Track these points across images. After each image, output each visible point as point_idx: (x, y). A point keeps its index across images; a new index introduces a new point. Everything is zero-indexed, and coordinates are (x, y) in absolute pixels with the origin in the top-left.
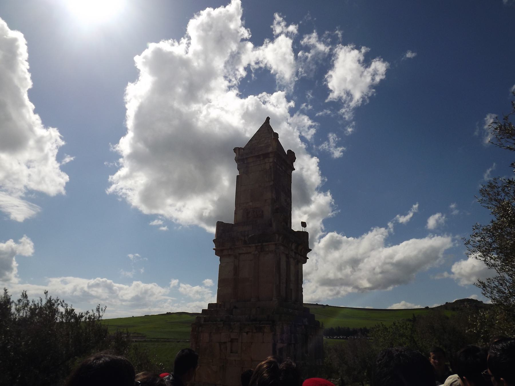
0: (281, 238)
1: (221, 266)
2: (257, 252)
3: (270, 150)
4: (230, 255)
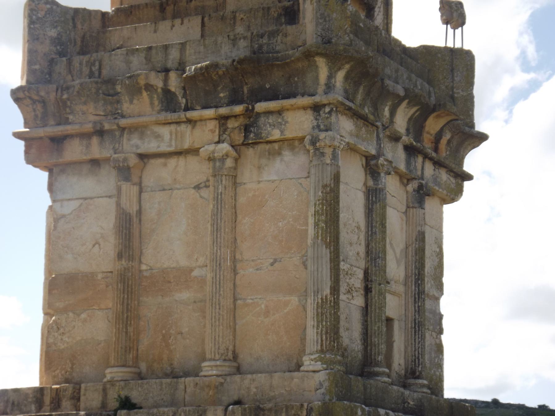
0: (340, 76)
2: (225, 147)
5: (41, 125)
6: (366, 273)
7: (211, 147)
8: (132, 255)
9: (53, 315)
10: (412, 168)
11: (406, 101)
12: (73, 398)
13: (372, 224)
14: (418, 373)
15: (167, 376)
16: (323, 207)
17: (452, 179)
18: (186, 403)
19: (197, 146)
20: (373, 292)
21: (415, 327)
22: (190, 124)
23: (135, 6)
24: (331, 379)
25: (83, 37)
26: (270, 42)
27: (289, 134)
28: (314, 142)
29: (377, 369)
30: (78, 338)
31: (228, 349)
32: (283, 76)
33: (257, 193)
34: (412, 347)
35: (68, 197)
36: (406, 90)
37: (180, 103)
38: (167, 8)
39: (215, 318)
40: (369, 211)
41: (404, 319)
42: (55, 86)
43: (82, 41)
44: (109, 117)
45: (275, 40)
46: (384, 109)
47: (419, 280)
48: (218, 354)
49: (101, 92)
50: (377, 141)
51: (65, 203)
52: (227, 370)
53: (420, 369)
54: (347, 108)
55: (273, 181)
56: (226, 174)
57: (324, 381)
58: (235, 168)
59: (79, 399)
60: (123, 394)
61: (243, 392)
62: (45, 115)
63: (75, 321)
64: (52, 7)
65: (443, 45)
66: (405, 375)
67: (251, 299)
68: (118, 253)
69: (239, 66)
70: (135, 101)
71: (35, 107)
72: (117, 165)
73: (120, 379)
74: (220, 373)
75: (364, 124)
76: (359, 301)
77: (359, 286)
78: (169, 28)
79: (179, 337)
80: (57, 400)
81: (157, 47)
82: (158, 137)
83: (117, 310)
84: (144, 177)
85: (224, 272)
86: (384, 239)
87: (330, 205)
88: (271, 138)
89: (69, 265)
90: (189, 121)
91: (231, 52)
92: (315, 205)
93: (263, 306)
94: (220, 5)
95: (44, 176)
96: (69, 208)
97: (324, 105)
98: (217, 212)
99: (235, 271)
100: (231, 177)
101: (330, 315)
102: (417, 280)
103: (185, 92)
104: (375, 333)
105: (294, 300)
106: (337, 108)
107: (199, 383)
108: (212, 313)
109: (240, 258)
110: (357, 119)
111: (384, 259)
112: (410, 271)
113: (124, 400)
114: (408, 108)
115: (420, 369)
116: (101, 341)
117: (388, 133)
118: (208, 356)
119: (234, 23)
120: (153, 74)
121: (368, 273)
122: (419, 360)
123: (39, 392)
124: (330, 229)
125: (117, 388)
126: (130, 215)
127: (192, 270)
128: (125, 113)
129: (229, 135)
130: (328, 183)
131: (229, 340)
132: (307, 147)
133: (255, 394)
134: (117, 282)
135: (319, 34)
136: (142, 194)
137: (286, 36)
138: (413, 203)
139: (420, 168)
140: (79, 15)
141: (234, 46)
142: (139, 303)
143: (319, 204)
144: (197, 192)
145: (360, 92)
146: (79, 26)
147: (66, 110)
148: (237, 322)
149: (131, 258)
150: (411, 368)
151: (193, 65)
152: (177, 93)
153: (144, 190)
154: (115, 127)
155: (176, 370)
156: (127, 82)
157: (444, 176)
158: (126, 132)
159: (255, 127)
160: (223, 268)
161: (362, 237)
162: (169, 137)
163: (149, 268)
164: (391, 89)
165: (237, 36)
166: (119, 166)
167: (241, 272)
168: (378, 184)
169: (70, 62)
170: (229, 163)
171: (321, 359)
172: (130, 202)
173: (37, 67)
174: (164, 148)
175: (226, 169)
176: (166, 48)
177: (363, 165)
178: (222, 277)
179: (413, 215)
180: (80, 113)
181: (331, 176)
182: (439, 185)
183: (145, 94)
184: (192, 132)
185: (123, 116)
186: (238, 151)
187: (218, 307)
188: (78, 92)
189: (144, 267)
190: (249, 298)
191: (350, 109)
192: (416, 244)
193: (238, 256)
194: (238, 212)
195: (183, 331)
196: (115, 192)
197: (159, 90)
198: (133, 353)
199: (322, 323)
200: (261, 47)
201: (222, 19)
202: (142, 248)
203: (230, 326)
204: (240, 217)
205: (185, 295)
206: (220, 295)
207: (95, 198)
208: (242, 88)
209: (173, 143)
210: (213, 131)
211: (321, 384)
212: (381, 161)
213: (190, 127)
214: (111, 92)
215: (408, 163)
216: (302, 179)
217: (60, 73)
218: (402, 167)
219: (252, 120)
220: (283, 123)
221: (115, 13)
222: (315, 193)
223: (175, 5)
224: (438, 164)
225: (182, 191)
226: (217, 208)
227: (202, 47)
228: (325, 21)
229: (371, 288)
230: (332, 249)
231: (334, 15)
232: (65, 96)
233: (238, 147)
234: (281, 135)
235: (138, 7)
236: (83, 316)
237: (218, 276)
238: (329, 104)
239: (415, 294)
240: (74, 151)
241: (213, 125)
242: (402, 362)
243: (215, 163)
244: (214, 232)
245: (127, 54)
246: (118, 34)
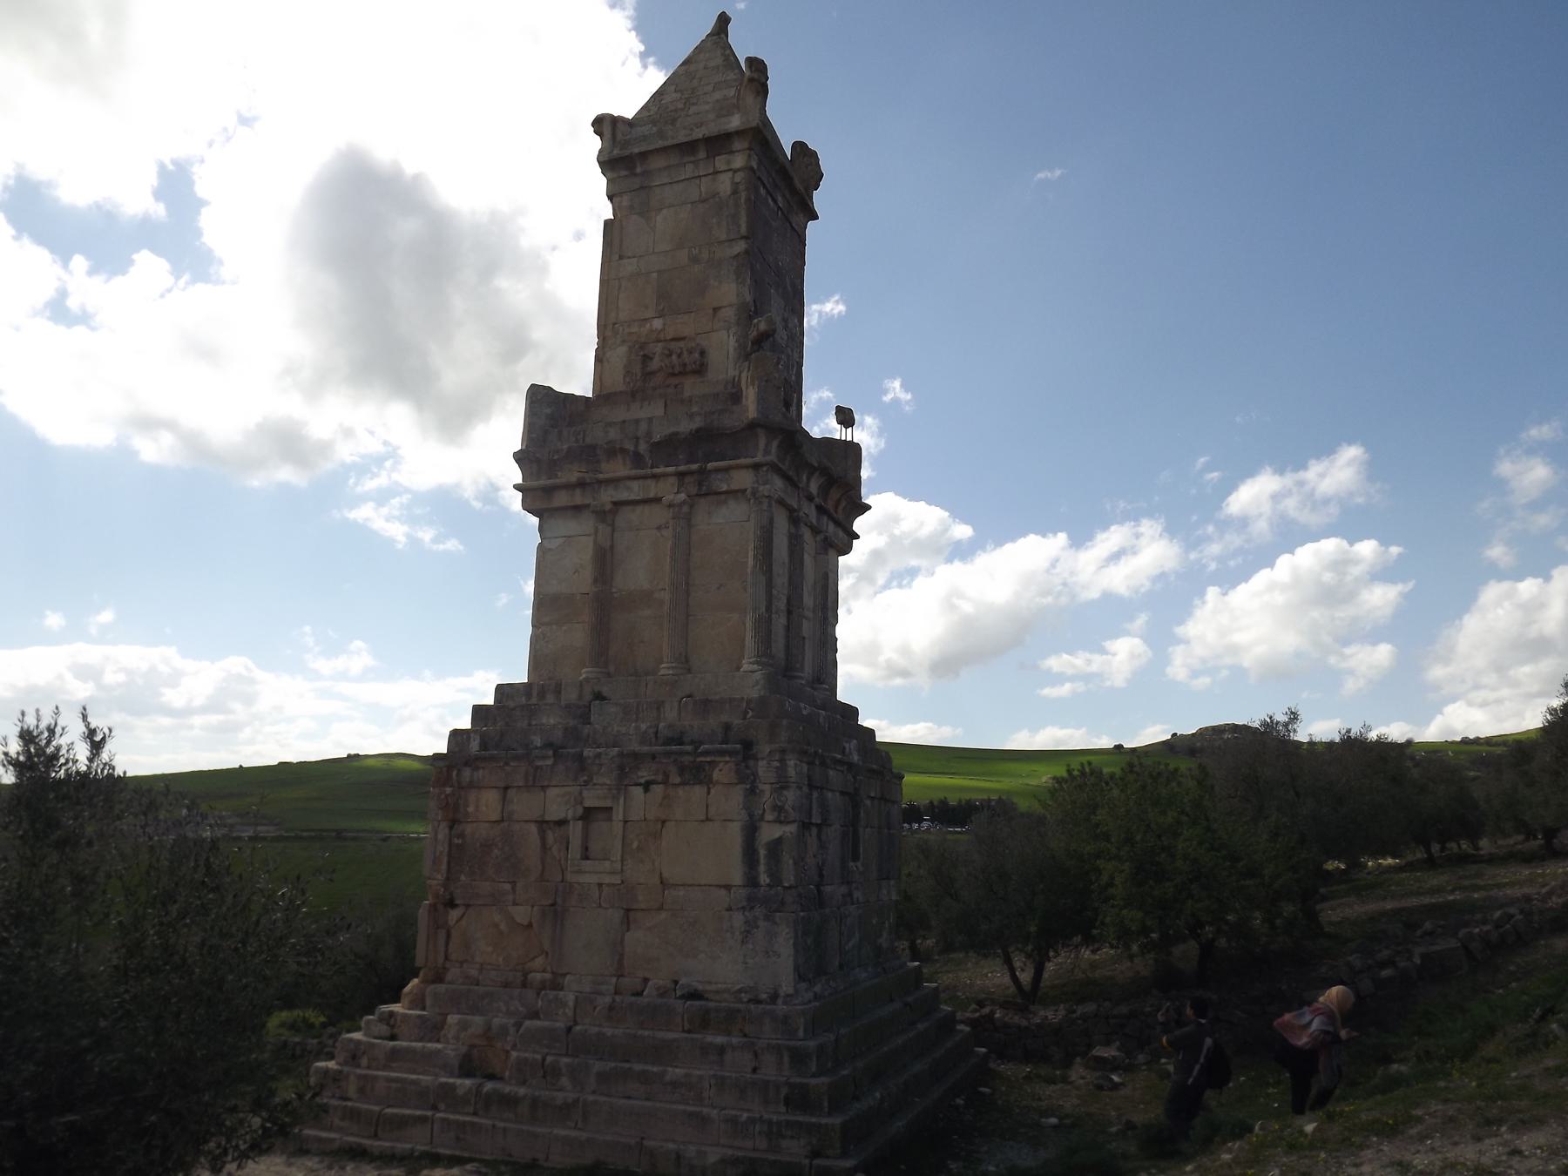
0: (775, 444)
3: (735, 122)
4: (578, 509)
27: (734, 486)
76: (783, 621)
90: (655, 477)
95: (535, 520)
123: (526, 688)
157: (841, 534)
170: (685, 509)
174: (633, 497)
176: (637, 421)
211: (757, 683)
215: (818, 519)
224: (837, 523)
240: (562, 499)
241: (673, 480)
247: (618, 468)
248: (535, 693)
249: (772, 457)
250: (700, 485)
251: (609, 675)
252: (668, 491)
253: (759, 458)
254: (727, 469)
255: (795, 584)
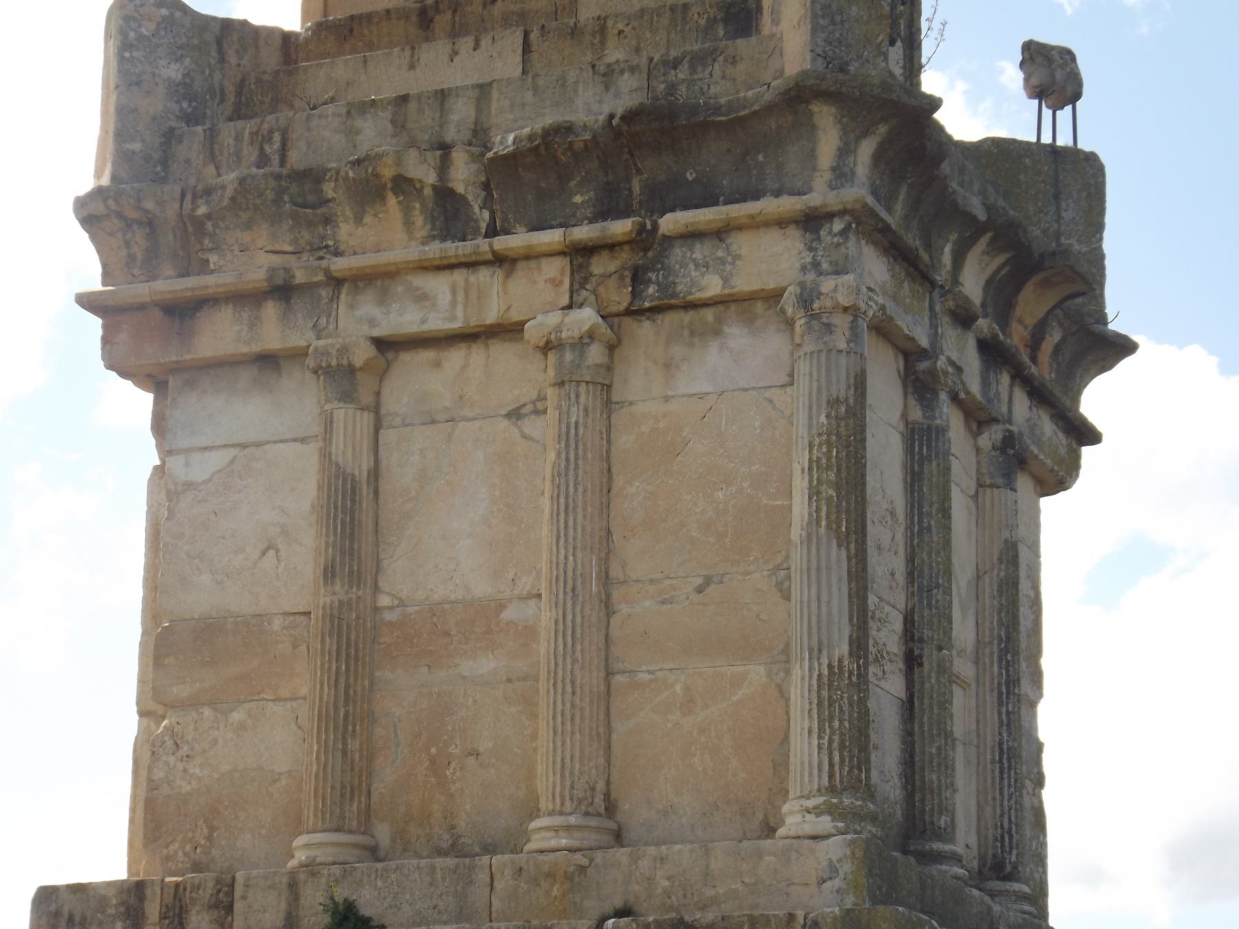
1: (167, 492)
2: (586, 317)
4: (268, 362)
5: (144, 278)
6: (909, 620)
7: (553, 319)
8: (359, 572)
9: (164, 718)
10: (992, 393)
11: (989, 235)
12: (215, 906)
13: (920, 507)
14: (1008, 868)
15: (441, 853)
16: (829, 451)
17: (1060, 435)
18: (494, 915)
19: (515, 316)
20: (926, 667)
21: (1001, 761)
22: (500, 266)
23: (360, 17)
24: (859, 854)
25: (241, 86)
26: (696, 77)
27: (743, 284)
28: (806, 300)
29: (937, 846)
30: (225, 768)
31: (593, 789)
32: (729, 150)
33: (661, 425)
34: (994, 808)
35: (203, 441)
36: (989, 208)
37: (476, 221)
38: (437, 18)
39: (562, 715)
40: (914, 479)
41: (975, 743)
42: (178, 188)
43: (239, 94)
44: (305, 257)
45: (707, 72)
46: (942, 249)
47: (1007, 652)
48: (571, 799)
49: (286, 198)
50: (931, 318)
51: (196, 457)
52: (592, 838)
53: (1013, 858)
54: (880, 226)
55: (702, 396)
56: (588, 379)
57: (840, 860)
58: (609, 368)
59: (230, 908)
60: (341, 894)
61: (637, 888)
62: (152, 254)
63: (218, 729)
64: (172, 15)
65: (1034, 140)
66: (980, 872)
67: (649, 672)
68: (325, 569)
69: (625, 128)
70: (368, 219)
71: (129, 236)
72: (324, 364)
73: (330, 859)
74: (576, 844)
75: (908, 274)
77: (896, 650)
78: (446, 59)
79: (471, 760)
80: (177, 911)
81: (419, 97)
82: (422, 298)
83: (321, 699)
84: (386, 391)
85: (583, 607)
86: (947, 544)
87: (847, 446)
88: (698, 295)
89: (202, 598)
90: (500, 260)
91: (600, 102)
92: (811, 446)
93: (678, 688)
94: (564, 8)
95: (145, 400)
96: (203, 467)
97: (830, 216)
98: (567, 468)
99: (608, 608)
100: (599, 387)
101: (851, 704)
102: (1003, 653)
103: (489, 195)
104: (931, 762)
105: (757, 673)
106: (858, 224)
107: (525, 868)
108: (555, 702)
109: (621, 576)
110: (895, 259)
111: (948, 591)
112: (987, 632)
113: (341, 907)
114: (988, 253)
115: (1013, 858)
116: (280, 774)
117: (951, 304)
118: (543, 805)
119: (603, 43)
120: (413, 153)
121: (913, 622)
122: (1011, 837)
124: (848, 503)
125: (323, 880)
126: (353, 480)
127: (501, 606)
128: (342, 247)
129: (594, 292)
130: (842, 394)
131: (597, 767)
132: (790, 311)
133: (667, 894)
134: (323, 634)
135: (819, 51)
136: (382, 431)
137: (734, 62)
138: (992, 476)
139: (1006, 400)
140: (232, 34)
141: (607, 88)
142: (372, 684)
143: (820, 445)
144: (515, 424)
145: (901, 197)
146: (233, 60)
147: (202, 244)
148: (613, 725)
149: (355, 578)
150: (994, 856)
151: (509, 131)
152: (470, 198)
153: (385, 424)
154: (320, 277)
155: (463, 840)
156: (351, 174)
157: (1048, 427)
158: (344, 291)
159: (658, 271)
160: (580, 598)
161: (900, 537)
162: (448, 297)
163: (396, 602)
164: (959, 201)
165: (616, 66)
166: (329, 366)
167: (624, 609)
168: (933, 418)
169: (212, 136)
170: (595, 354)
171: (830, 810)
172: (354, 449)
173: (137, 146)
174: (437, 323)
175: (588, 367)
176: (442, 96)
177: (899, 371)
178: (578, 620)
179: (993, 505)
180: (236, 248)
181: (848, 379)
182: (1039, 443)
183: (392, 201)
184: (504, 285)
185: (337, 253)
186: (616, 328)
187: (569, 689)
188: (233, 199)
189: (384, 601)
190: (644, 668)
191: (885, 229)
192: (1000, 569)
193: (615, 572)
194: (614, 470)
195: (481, 749)
196: (317, 429)
197: (428, 191)
198: (360, 802)
199: (831, 722)
200: (672, 88)
201: (572, 34)
202: (381, 556)
203: (598, 734)
204: (619, 481)
205: (486, 665)
206: (574, 661)
207: (268, 442)
208: (628, 180)
209: (460, 312)
210: (556, 283)
212: (941, 363)
213: (500, 273)
214: (311, 198)
215: (985, 383)
216: (773, 390)
217: (188, 161)
218: (975, 387)
219: (650, 254)
220: (730, 259)
221: (314, 33)
222: (810, 418)
223: (455, 11)
224: (1039, 395)
225: (477, 423)
226: (567, 460)
227: (530, 93)
228: (833, 22)
229: (921, 656)
230: (853, 551)
231: (854, 11)
232: (202, 210)
233: (616, 320)
234: (724, 288)
235: (369, 17)
236: (236, 716)
237: (569, 617)
238: (842, 213)
239: (999, 684)
240: (221, 334)
241: (556, 268)
242: (973, 840)
243: (562, 356)
244: (558, 514)
245: (349, 112)
246: (321, 77)
247: (388, 236)
248: (153, 910)
249: (857, 192)
250: (638, 277)
251: (373, 852)
252: (537, 296)
253: (819, 196)
254: (720, 233)
255: (926, 576)
